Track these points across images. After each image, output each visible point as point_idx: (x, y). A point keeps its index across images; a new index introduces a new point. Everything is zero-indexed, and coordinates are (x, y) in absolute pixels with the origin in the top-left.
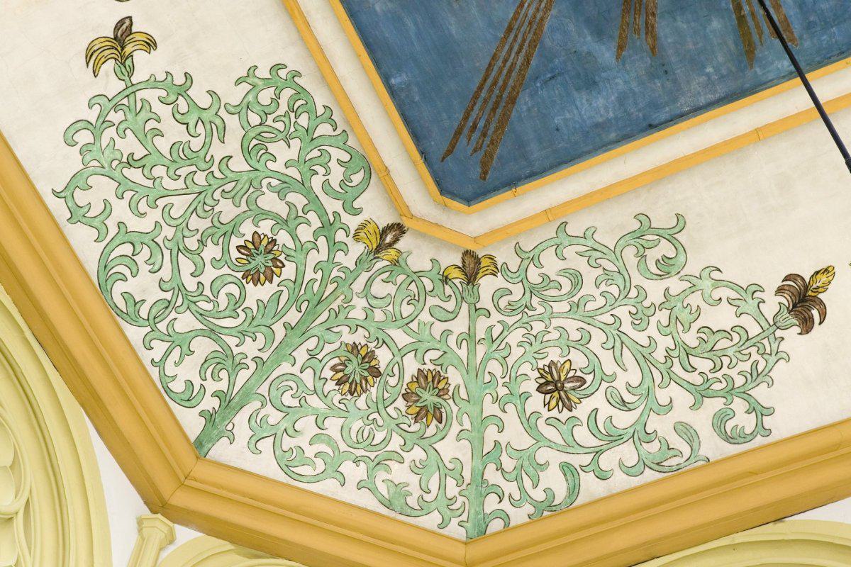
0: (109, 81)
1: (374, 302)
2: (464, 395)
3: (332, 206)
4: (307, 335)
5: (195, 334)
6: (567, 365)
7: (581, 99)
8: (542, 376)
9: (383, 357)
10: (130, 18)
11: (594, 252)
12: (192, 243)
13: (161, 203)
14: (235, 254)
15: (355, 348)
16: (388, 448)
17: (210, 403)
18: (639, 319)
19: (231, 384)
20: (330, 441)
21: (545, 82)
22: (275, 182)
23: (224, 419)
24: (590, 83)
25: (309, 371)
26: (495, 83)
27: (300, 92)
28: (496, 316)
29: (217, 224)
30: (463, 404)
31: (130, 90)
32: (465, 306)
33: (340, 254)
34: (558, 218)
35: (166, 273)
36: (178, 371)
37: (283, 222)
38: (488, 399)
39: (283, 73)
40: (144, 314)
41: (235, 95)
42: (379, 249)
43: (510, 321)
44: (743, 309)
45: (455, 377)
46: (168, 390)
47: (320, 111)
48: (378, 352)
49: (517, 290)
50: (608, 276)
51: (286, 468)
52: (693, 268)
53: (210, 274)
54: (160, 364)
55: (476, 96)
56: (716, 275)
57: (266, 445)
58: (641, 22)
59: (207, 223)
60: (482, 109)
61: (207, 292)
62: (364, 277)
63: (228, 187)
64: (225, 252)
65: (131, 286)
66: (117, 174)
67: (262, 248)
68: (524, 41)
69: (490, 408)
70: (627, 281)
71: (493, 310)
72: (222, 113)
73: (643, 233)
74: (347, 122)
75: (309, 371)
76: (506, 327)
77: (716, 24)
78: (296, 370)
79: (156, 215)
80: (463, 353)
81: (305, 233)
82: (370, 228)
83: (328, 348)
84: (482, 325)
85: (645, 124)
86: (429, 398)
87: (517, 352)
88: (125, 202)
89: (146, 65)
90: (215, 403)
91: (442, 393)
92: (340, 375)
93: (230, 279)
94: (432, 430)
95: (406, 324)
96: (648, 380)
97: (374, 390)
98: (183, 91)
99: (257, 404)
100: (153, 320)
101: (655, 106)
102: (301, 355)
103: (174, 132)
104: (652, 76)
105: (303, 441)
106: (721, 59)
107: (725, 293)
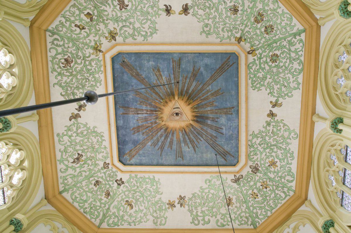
0: (281, 100)
1: (259, 41)
2: (252, 15)
3: (257, 62)
4: (274, 40)
5: (292, 52)
6: (231, 13)
7: (209, 63)
8: (237, 13)
9: (263, 30)
10: (272, 107)
12: (284, 68)
13: (284, 77)
14: (278, 62)
15: (267, 34)
16: (271, 12)
17: (298, 37)
18: (215, 17)
19: (292, 39)
20: (281, 19)
21: (213, 68)
22: (264, 71)
23: (297, 33)
24: (206, 65)
25: (277, 33)
26: (221, 72)
27: (252, 84)
28: (240, 28)
29: (278, 68)
30: (254, 13)
31: (278, 97)
32: (244, 33)
33: (260, 53)
34: (221, 44)
35: (291, 65)
36: (300, 47)
37: (267, 63)
38: (248, 12)
39: (253, 88)
40: (299, 61)
42: (254, 50)
43: (238, 26)
44: (196, 12)
45: (252, 19)
46: (303, 45)
47: (251, 80)
48: (264, 31)
49: (234, 32)
51: (291, 18)
52: (202, 23)
53: (284, 61)
54: (301, 50)
55: (225, 71)
56: (199, 20)
57: (293, 24)
58: (195, 72)
59: (279, 69)
60: (225, 69)
61: (286, 58)
62: (259, 46)
63: (273, 74)
64: (279, 63)
65: (298, 67)
66: (288, 86)
67: (273, 60)
68: (214, 77)
69: (249, 10)
70: (214, 26)
71: (240, 30)
72: (266, 86)
73: (208, 34)
74: (247, 76)
75: (277, 33)
76: (239, 25)
77: (183, 67)
78: (279, 35)
79: (287, 76)
80: (249, 23)
81: (264, 59)
82: (253, 55)
83: (272, 36)
84: (243, 28)
85: (200, 54)
86: (259, 18)
87: (239, 20)
88: (290, 81)
89: (274, 100)
90: (297, 37)
91: (256, 18)
92: (272, 30)
93: (281, 58)
94: (262, 11)
96: (218, 5)
97: (268, 24)
98: (270, 93)
99: (290, 32)
100: (298, 59)
101: (198, 57)
102: (277, 37)
103: (276, 87)
104: (196, 62)
105: (286, 21)
106: (185, 60)
107: (198, 17)
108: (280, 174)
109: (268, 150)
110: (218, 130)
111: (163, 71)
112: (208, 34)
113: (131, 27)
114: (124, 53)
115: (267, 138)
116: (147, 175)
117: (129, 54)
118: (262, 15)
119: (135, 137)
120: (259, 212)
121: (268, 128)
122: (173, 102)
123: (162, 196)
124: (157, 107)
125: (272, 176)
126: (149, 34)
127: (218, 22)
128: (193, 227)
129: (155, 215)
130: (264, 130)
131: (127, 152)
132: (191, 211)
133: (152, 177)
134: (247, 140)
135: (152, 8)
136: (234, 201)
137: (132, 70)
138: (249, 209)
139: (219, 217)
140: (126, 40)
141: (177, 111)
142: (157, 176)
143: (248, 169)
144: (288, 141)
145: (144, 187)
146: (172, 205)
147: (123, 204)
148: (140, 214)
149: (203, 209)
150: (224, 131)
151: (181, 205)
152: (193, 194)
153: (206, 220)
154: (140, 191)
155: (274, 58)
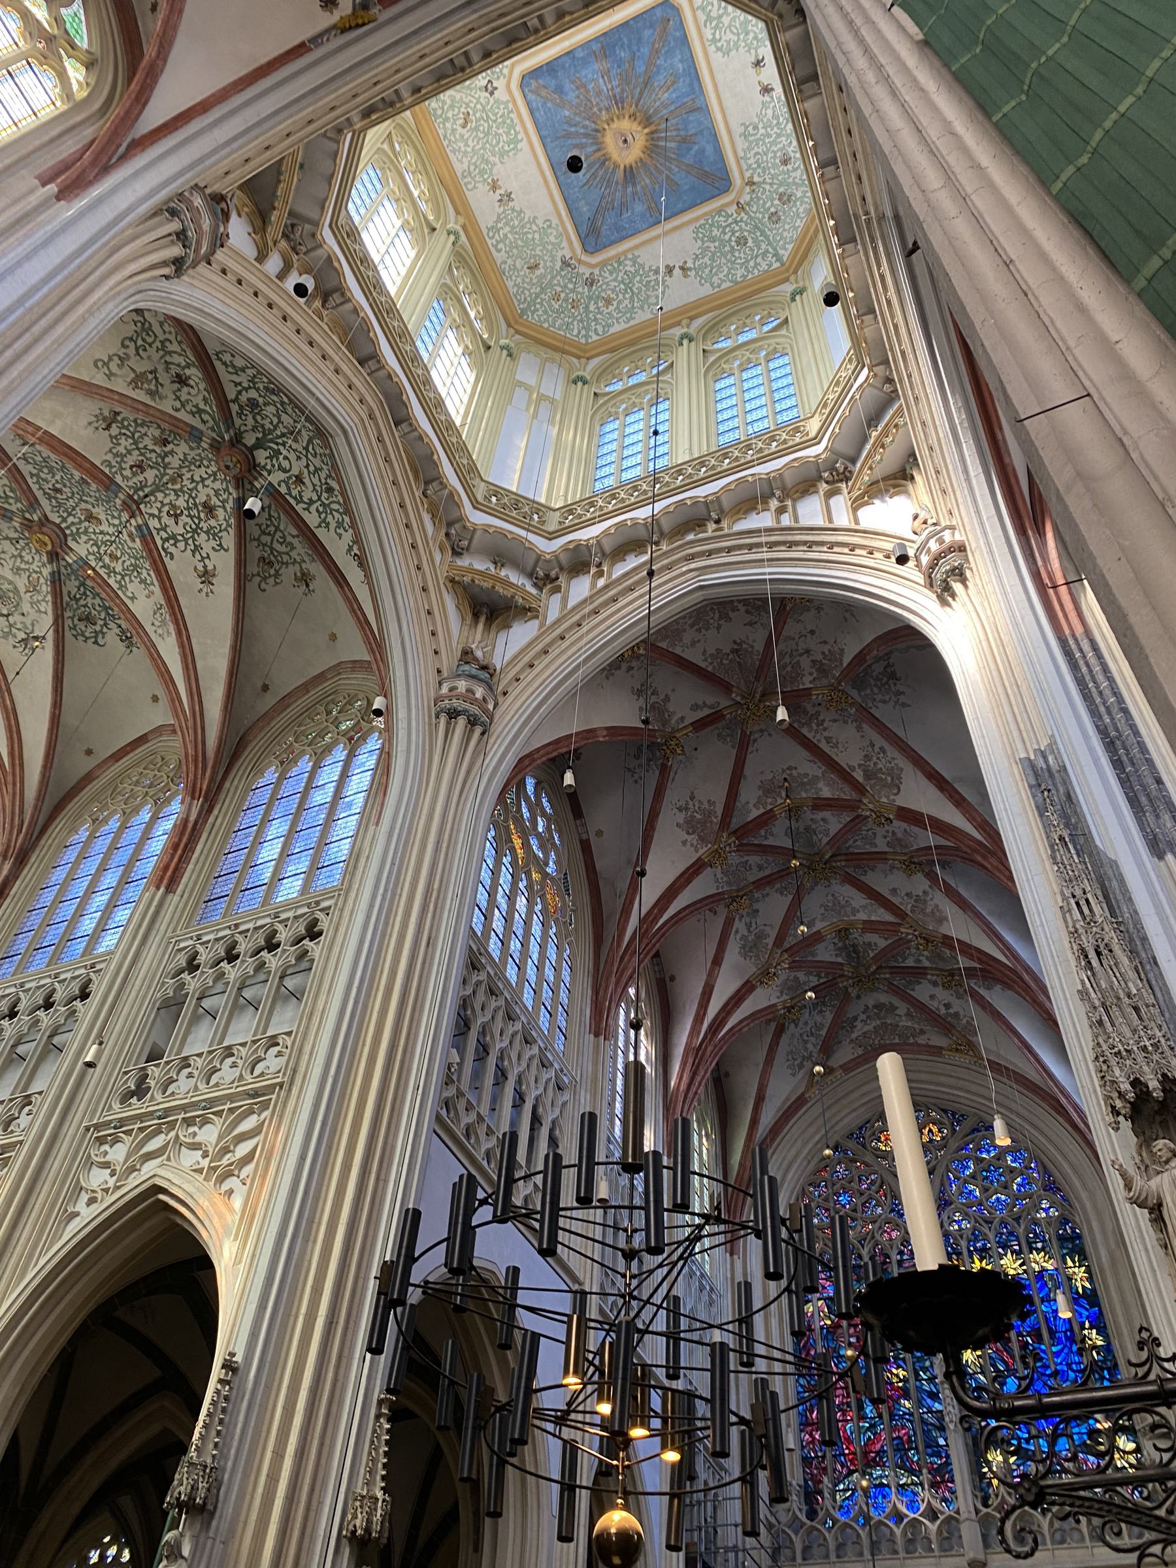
0: (692, 273)
3: (730, 220)
9: (773, 210)
11: (749, 149)
18: (769, 136)
24: (703, 151)
37: (733, 234)
41: (700, 242)
45: (781, 190)
49: (759, 170)
50: (757, 144)
69: (791, 180)
73: (745, 135)
81: (737, 228)
84: (768, 181)
86: (785, 198)
89: (690, 264)
95: (765, 203)
103: (706, 259)
108: (599, 316)
109: (622, 286)
110: (624, 206)
111: (674, 91)
112: (745, 135)
113: (721, 11)
114: (679, 15)
115: (638, 278)
116: (518, 128)
117: (681, 26)
118: (789, 201)
119: (568, 86)
120: (540, 313)
121: (651, 274)
122: (639, 128)
123: (499, 165)
124: (622, 103)
125: (592, 308)
126: (719, 45)
127: (764, 143)
128: (485, 231)
129: (472, 168)
130: (647, 269)
131: (541, 82)
132: (499, 220)
133: (519, 137)
134: (625, 252)
135: (755, 38)
136: (538, 272)
137: (661, 39)
138: (536, 298)
139: (509, 261)
140: (699, 13)
141: (630, 139)
142: (523, 145)
143: (585, 271)
144: (646, 306)
145: (501, 131)
146: (494, 187)
147: (463, 110)
148: (462, 145)
149: (509, 235)
150: (625, 216)
151: (500, 201)
152: (521, 211)
153: (501, 246)
154: (490, 127)
155: (741, 242)
